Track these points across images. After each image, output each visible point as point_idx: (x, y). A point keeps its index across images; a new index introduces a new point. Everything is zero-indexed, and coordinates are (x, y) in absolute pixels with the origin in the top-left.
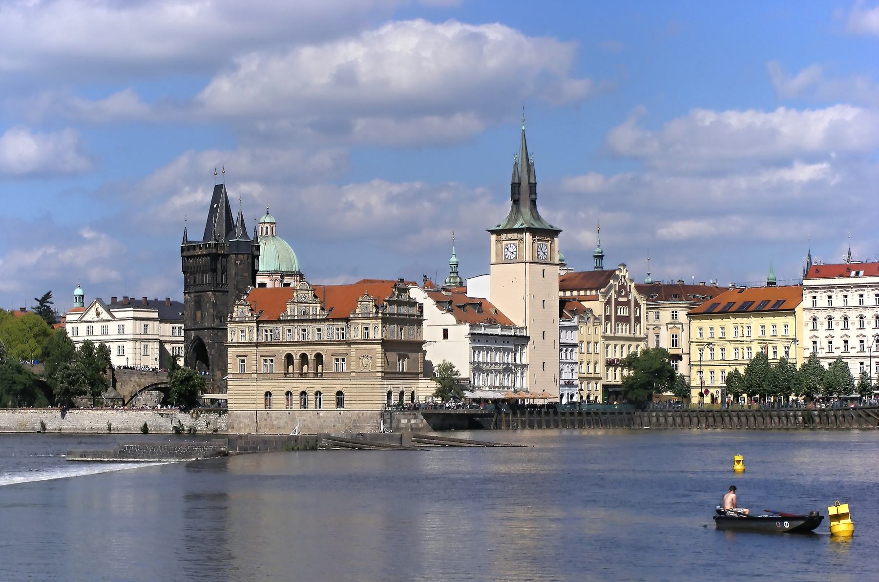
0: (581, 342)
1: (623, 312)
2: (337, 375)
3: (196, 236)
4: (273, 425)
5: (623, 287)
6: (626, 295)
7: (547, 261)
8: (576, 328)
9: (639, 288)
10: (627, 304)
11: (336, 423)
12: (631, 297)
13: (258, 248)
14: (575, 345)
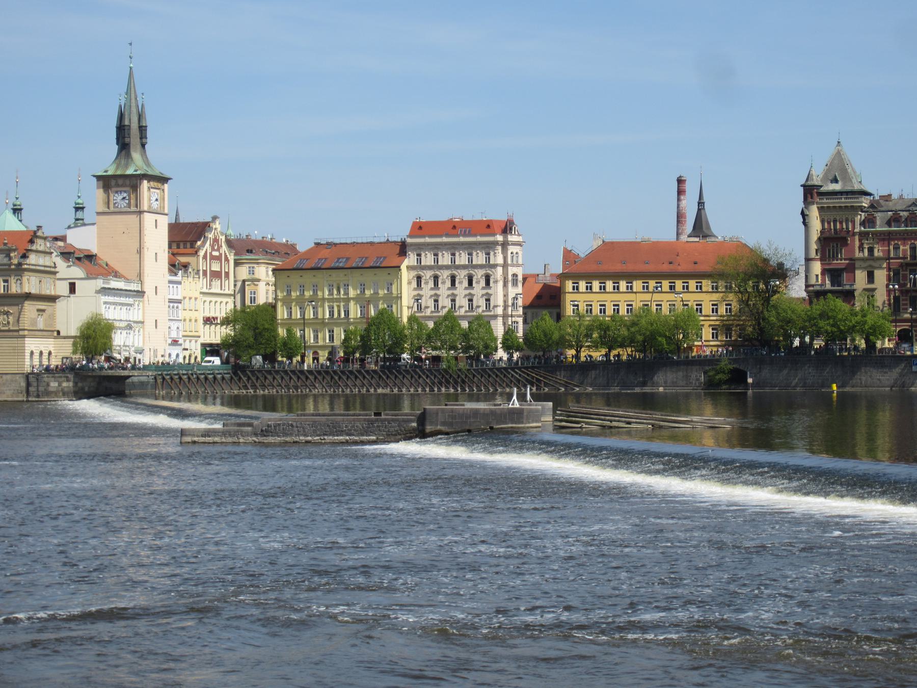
0: (185, 298)
1: (216, 267)
5: (216, 240)
6: (218, 250)
7: (159, 211)
8: (180, 283)
9: (229, 243)
10: (218, 258)
12: (222, 251)
14: (179, 302)
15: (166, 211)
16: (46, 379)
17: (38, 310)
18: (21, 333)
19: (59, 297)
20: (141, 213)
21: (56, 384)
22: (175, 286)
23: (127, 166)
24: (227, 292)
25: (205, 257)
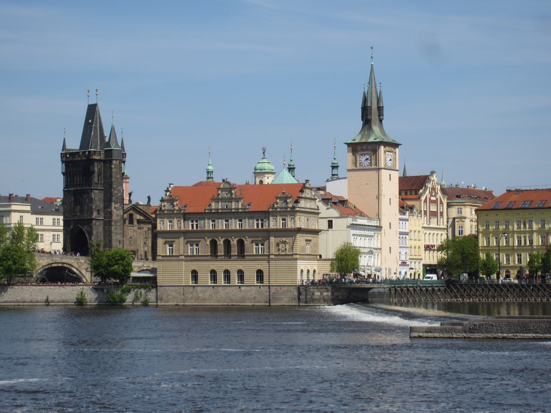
0: (411, 231)
1: (433, 208)
2: (256, 257)
3: (74, 144)
4: (199, 297)
5: (433, 189)
6: (435, 196)
7: (392, 168)
8: (407, 220)
9: (443, 191)
10: (435, 202)
11: (256, 296)
12: (438, 197)
13: (124, 155)
14: (407, 234)
15: (397, 168)
16: (312, 290)
17: (306, 240)
18: (294, 256)
19: (321, 231)
20: (379, 169)
21: (319, 294)
22: (404, 222)
23: (369, 136)
24: (441, 226)
25: (425, 201)
